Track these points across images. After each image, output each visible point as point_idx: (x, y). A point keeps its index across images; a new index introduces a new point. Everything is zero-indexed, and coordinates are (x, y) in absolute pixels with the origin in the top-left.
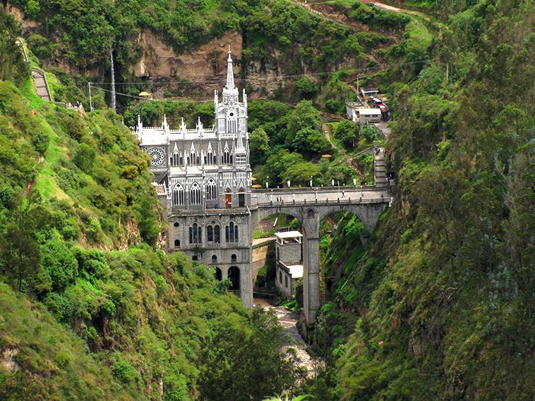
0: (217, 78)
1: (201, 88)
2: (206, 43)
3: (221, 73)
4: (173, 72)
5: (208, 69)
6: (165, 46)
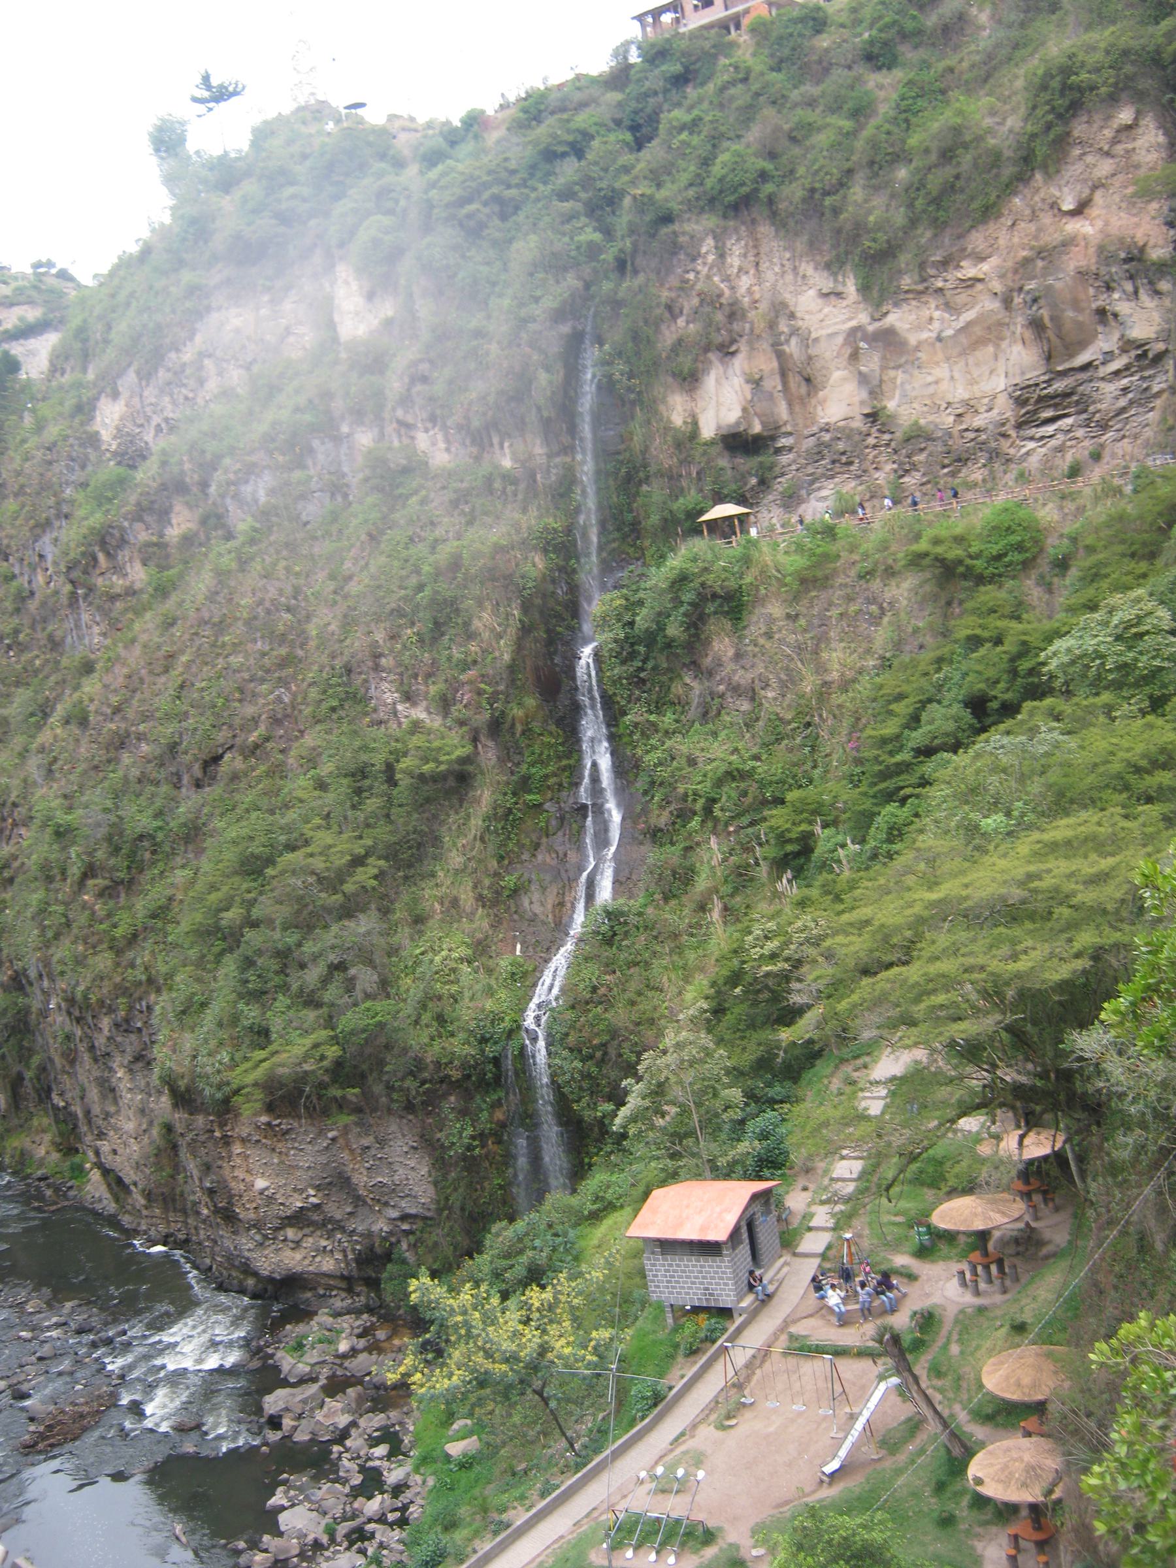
0: (1059, 386)
1: (994, 455)
2: (988, 213)
5: (1018, 348)
6: (824, 282)
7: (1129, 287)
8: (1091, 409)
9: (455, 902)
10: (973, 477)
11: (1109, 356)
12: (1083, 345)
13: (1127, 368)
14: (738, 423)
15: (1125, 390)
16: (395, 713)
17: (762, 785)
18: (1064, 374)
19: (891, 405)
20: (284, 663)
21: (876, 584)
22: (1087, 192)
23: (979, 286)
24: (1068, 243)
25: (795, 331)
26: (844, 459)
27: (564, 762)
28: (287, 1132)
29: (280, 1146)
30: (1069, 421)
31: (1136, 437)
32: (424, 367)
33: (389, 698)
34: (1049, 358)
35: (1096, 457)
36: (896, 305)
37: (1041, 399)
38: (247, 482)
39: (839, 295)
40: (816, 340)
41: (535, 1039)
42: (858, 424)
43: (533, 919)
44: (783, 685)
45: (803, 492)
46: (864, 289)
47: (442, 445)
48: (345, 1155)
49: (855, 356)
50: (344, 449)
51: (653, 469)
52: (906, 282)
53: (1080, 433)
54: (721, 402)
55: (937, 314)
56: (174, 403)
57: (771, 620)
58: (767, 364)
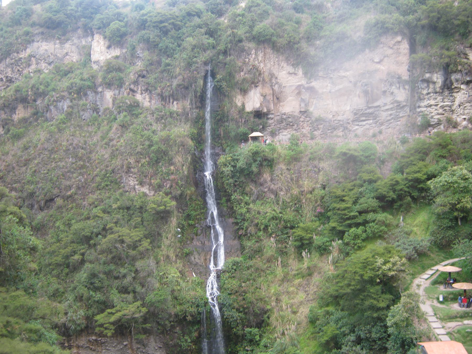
0: (370, 111)
1: (346, 128)
3: (376, 104)
4: (303, 105)
6: (291, 69)
7: (398, 85)
8: (378, 119)
9: (168, 257)
10: (339, 134)
11: (385, 104)
12: (376, 100)
13: (391, 108)
14: (259, 108)
15: (391, 115)
16: (135, 189)
17: (286, 222)
18: (370, 108)
19: (311, 109)
20: (82, 167)
21: (316, 162)
22: (382, 58)
23: (345, 79)
24: (377, 71)
25: (277, 83)
26: (291, 124)
27: (202, 211)
28: (104, 343)
29: (99, 349)
30: (371, 121)
31: (394, 128)
32: (145, 73)
33: (132, 183)
34: (368, 102)
35: (380, 132)
36: (315, 80)
37: (363, 114)
38: (60, 102)
39: (295, 74)
40: (284, 87)
41: (214, 306)
42: (297, 114)
43: (196, 264)
44: (287, 190)
45: (277, 133)
46: (305, 74)
47: (148, 99)
49: (299, 93)
50: (99, 96)
51: (230, 117)
52: (321, 74)
53: (374, 125)
54: (253, 101)
55: (329, 85)
56: (13, 71)
57: (282, 170)
58: (268, 91)
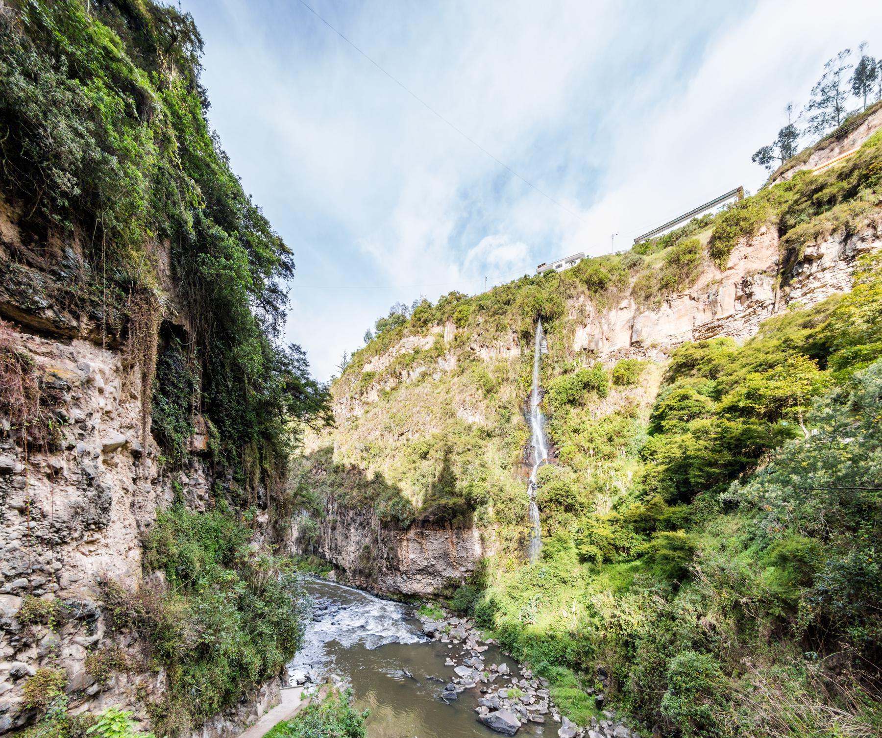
29: (424, 542)
48: (450, 545)
